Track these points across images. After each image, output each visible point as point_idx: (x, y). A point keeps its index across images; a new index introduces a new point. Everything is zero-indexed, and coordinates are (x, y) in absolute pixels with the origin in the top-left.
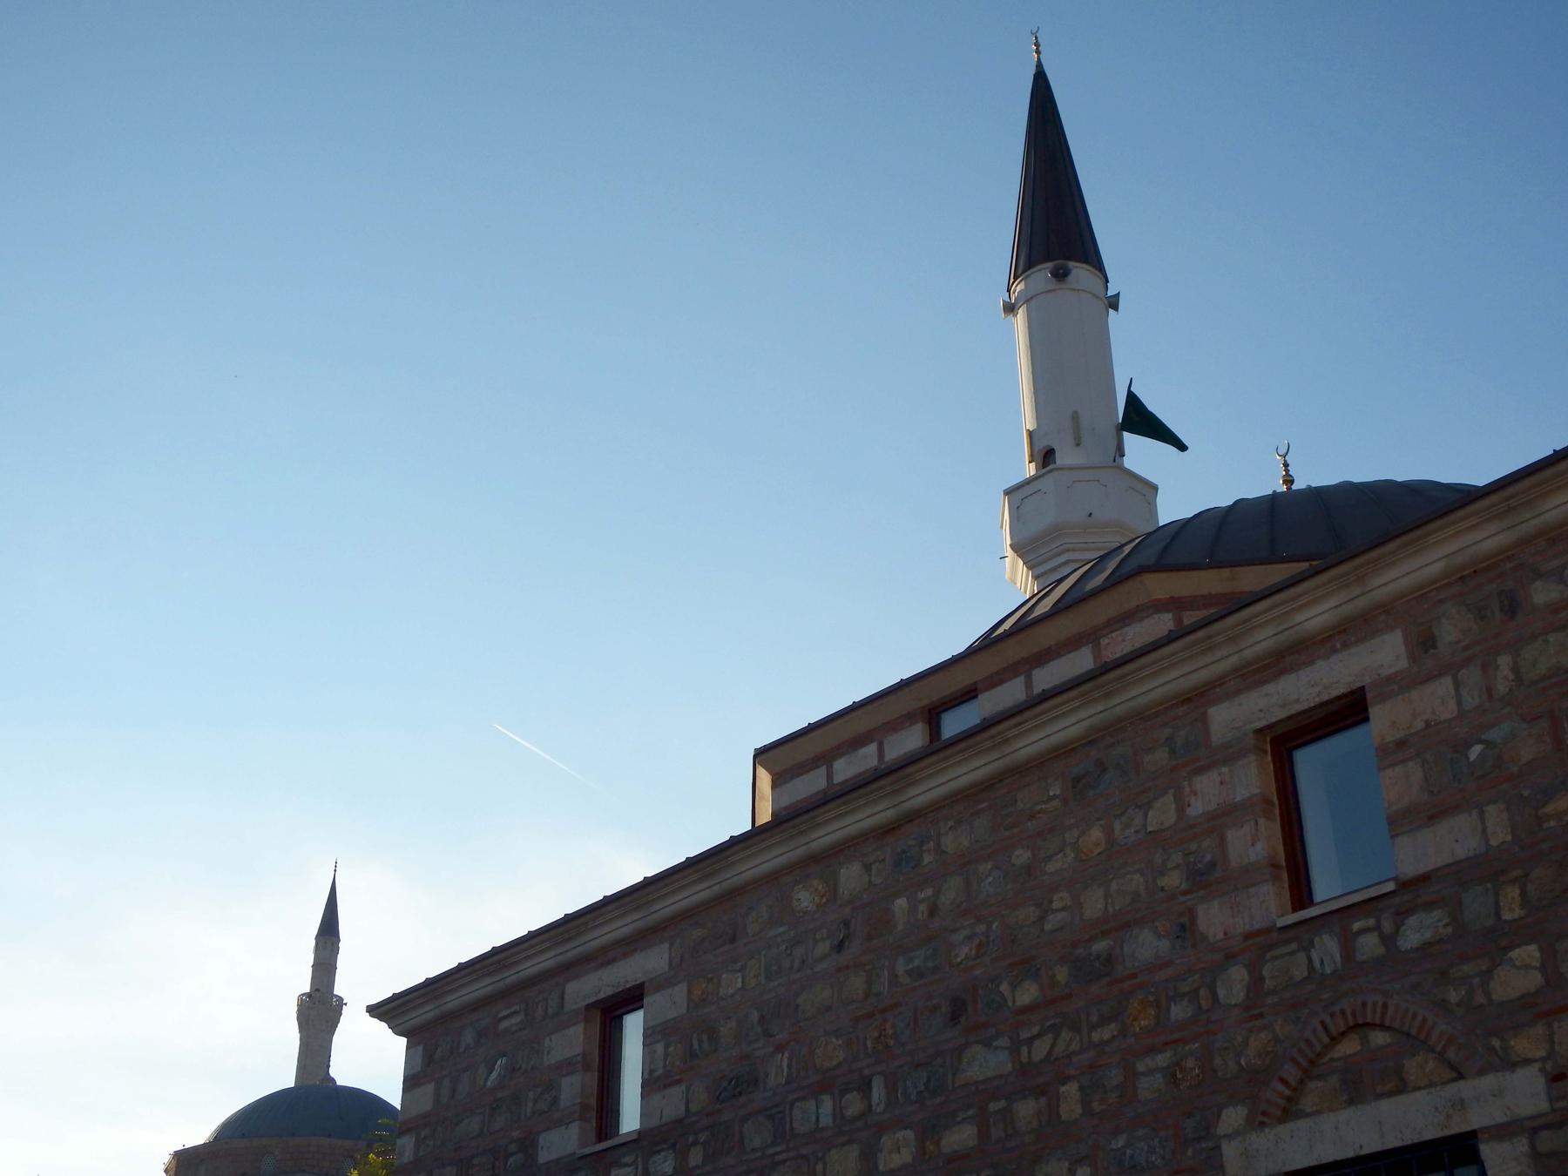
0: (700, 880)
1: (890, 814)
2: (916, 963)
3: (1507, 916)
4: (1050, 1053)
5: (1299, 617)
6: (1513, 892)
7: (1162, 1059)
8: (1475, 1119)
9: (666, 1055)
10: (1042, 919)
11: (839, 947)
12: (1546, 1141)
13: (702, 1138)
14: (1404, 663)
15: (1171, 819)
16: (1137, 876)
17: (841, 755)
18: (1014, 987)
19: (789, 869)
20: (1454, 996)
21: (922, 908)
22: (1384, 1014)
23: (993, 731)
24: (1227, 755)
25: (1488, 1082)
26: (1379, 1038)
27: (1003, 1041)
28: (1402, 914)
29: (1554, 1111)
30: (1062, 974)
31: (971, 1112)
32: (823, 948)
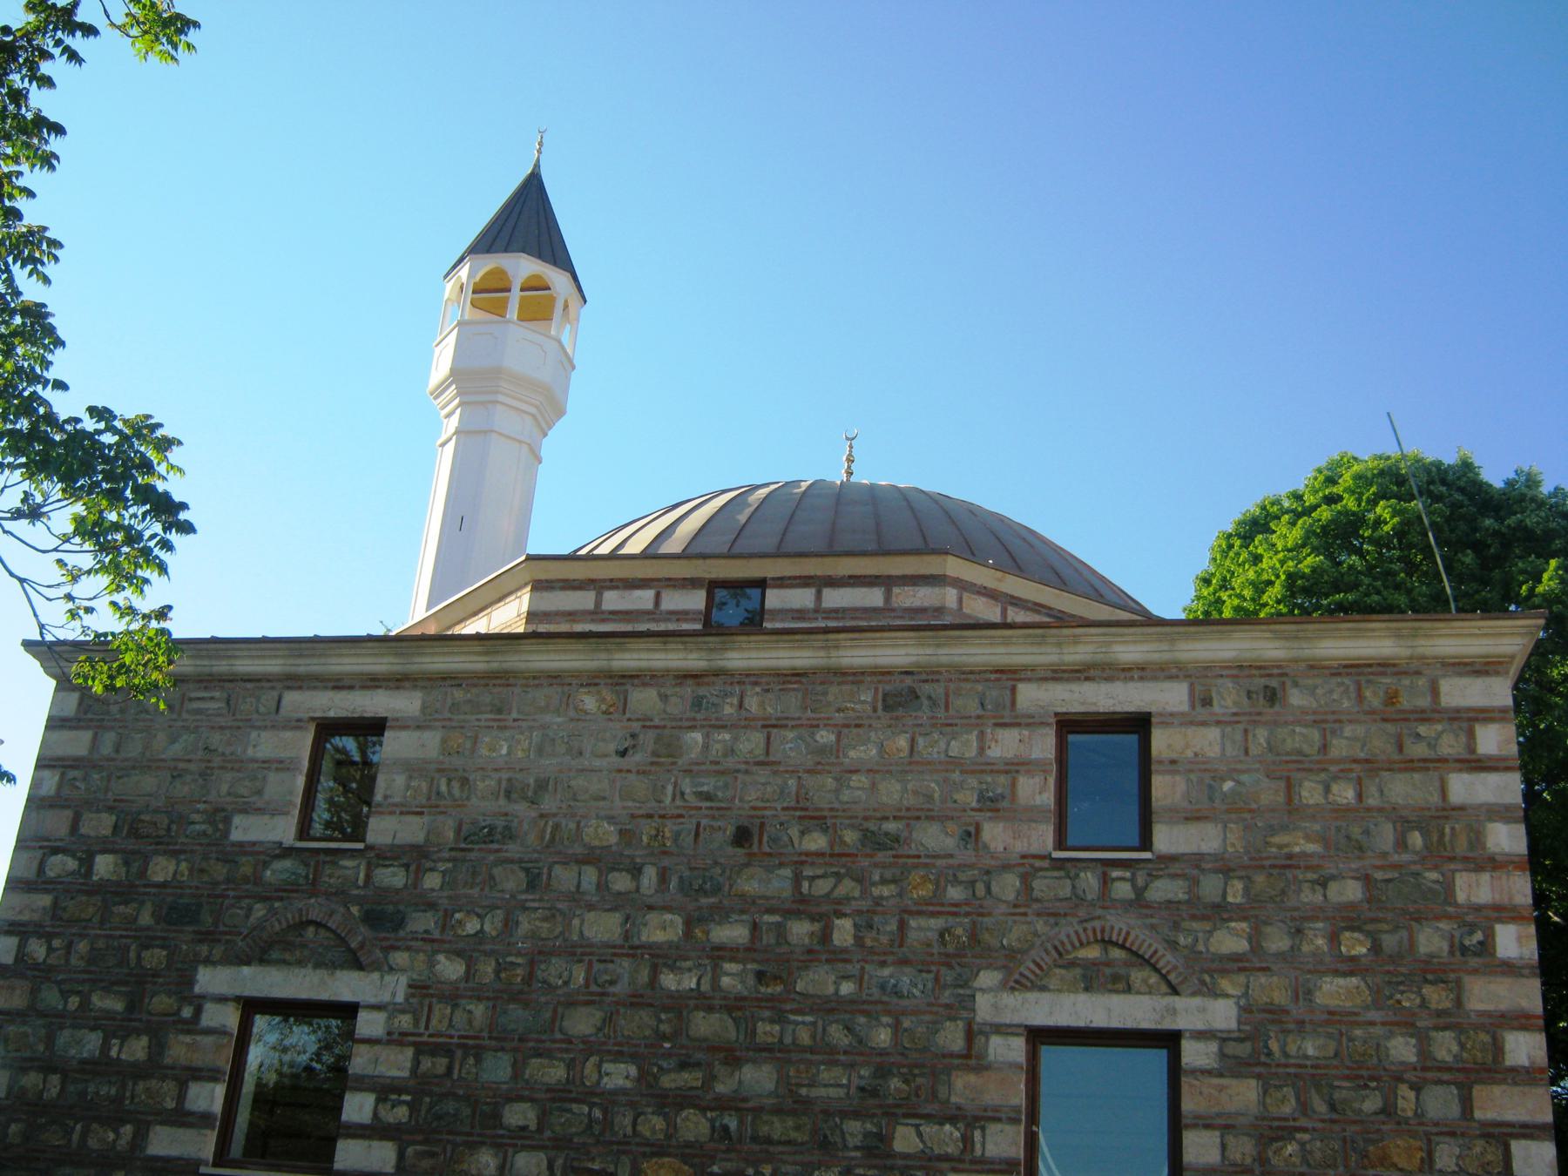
0: (479, 654)
1: (702, 664)
2: (705, 788)
3: (1230, 899)
4: (828, 895)
7: (937, 923)
8: (1180, 1023)
9: (408, 787)
10: (837, 791)
11: (623, 753)
12: (1232, 1048)
13: (442, 866)
14: (1185, 708)
15: (972, 752)
17: (616, 588)
18: (803, 833)
20: (1182, 940)
21: (716, 749)
22: (1125, 939)
23: (831, 636)
26: (1116, 953)
27: (787, 872)
28: (1152, 877)
30: (850, 837)
31: (744, 917)
32: (612, 747)
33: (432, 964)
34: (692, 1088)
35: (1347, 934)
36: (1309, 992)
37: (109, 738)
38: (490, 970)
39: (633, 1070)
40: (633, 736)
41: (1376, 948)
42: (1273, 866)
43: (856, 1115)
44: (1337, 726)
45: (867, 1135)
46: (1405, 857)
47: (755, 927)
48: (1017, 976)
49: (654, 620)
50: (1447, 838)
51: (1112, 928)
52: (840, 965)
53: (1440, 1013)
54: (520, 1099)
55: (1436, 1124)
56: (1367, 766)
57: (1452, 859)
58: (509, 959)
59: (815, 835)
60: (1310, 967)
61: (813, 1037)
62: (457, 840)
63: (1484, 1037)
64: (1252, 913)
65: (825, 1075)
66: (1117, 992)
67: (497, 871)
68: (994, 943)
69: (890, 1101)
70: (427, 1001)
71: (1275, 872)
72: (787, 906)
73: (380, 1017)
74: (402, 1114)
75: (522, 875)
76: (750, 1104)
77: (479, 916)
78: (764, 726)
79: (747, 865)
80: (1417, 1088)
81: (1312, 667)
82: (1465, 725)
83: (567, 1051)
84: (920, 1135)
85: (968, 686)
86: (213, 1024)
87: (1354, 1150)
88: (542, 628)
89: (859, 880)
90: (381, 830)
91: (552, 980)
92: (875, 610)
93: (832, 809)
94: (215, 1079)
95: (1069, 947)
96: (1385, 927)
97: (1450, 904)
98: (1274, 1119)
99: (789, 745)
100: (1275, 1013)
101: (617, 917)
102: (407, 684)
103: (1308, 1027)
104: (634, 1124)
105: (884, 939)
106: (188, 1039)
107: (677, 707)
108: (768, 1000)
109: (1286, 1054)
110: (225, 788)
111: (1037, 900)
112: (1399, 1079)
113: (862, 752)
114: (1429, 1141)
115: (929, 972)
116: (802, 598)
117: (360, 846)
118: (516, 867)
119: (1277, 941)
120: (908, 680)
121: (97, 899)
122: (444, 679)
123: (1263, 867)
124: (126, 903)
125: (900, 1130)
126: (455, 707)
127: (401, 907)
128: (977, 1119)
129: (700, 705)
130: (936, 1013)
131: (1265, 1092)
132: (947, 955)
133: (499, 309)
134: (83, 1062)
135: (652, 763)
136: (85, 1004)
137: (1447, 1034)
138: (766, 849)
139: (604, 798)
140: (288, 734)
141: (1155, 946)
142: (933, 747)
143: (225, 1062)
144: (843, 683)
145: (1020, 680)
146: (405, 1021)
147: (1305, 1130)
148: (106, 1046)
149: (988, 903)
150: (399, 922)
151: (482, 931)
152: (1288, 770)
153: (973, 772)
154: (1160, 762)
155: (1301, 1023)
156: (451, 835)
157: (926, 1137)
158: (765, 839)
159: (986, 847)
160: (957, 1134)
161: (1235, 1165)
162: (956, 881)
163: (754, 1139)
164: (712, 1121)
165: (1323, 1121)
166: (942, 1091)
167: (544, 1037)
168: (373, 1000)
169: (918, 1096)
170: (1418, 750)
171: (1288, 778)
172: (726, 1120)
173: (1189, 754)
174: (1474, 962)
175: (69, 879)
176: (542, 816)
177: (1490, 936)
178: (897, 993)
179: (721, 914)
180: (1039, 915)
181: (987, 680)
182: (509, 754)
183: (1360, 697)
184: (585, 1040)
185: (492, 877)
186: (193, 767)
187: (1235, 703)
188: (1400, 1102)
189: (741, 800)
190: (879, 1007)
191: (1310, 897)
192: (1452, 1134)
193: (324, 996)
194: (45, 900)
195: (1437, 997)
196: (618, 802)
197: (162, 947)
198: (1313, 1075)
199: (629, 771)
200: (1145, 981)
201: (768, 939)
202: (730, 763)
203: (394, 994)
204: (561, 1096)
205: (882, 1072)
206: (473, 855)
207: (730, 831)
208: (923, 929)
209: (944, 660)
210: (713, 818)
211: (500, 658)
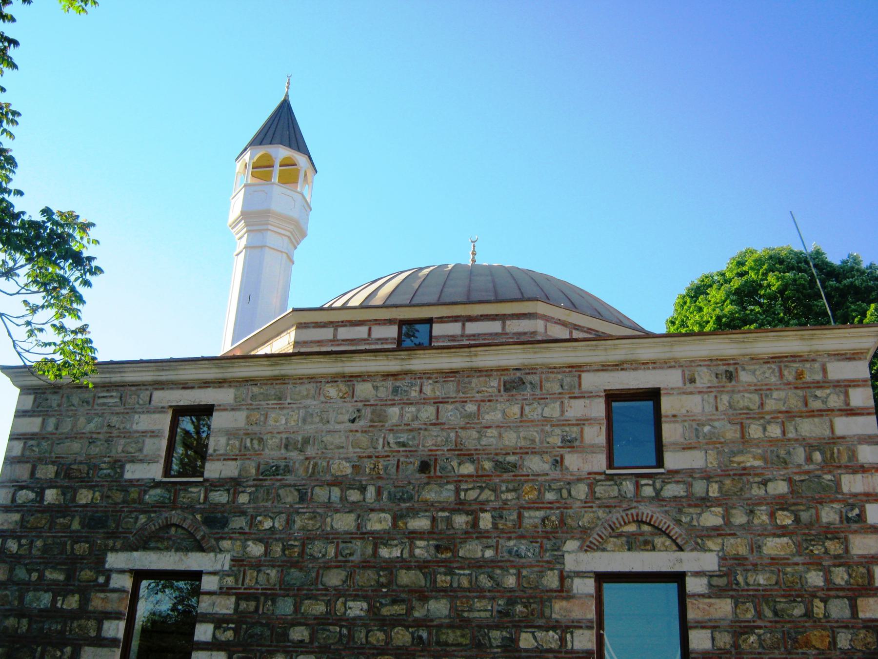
2: (402, 440)
5: (639, 351)
6: (715, 486)
7: (540, 514)
9: (228, 444)
10: (479, 439)
11: (353, 421)
13: (249, 490)
14: (680, 384)
15: (556, 414)
16: (535, 434)
18: (460, 464)
19: (324, 376)
20: (684, 520)
21: (408, 417)
22: (651, 520)
23: (473, 349)
24: (589, 396)
25: (695, 554)
26: (646, 528)
27: (451, 487)
29: (719, 570)
30: (488, 465)
31: (427, 514)
32: (346, 417)
33: (245, 547)
34: (400, 615)
35: (780, 512)
36: (759, 547)
37: (52, 421)
38: (279, 549)
39: (365, 606)
40: (358, 411)
41: (797, 520)
42: (735, 475)
43: (497, 627)
44: (768, 392)
45: (503, 639)
46: (812, 467)
47: (434, 520)
48: (588, 543)
49: (368, 344)
50: (835, 455)
51: (643, 514)
52: (485, 540)
53: (837, 557)
54: (300, 624)
55: (837, 622)
56: (787, 415)
57: (839, 467)
58: (290, 543)
59: (467, 465)
60: (759, 532)
61: (470, 582)
62: (257, 474)
63: (862, 570)
64: (724, 502)
65: (478, 605)
66: (647, 550)
67: (281, 492)
68: (574, 524)
69: (517, 619)
70: (242, 569)
71: (736, 478)
72: (452, 506)
73: (216, 579)
74: (229, 635)
75: (296, 493)
76: (435, 623)
77: (271, 518)
78: (435, 403)
79: (428, 483)
80: (825, 601)
81: (753, 359)
82: (843, 389)
83: (326, 595)
84: (535, 638)
85: (553, 376)
86: (116, 586)
87: (790, 638)
88: (302, 350)
89: (494, 490)
90: (213, 470)
91: (315, 554)
92: (496, 334)
93: (476, 450)
94: (119, 619)
95: (618, 525)
96: (802, 507)
97: (839, 493)
98: (742, 622)
99: (449, 413)
100: (740, 560)
101: (352, 517)
102: (226, 385)
103: (759, 567)
104: (367, 637)
105: (510, 524)
106: (102, 595)
107: (383, 393)
108: (442, 562)
109: (747, 584)
110: (120, 449)
111: (598, 499)
112: (814, 596)
113: (493, 416)
114: (833, 632)
115: (537, 542)
116: (454, 329)
117: (201, 479)
118: (292, 489)
119: (739, 518)
120: (518, 374)
121: (47, 515)
122: (247, 381)
123: (729, 475)
124: (64, 517)
125: (523, 636)
126: (254, 397)
127: (226, 515)
128: (568, 627)
129: (397, 391)
130: (542, 566)
131: (736, 607)
132: (547, 532)
133: (267, 178)
134: (41, 610)
135: (371, 426)
136: (41, 577)
137: (841, 568)
138: (438, 474)
139: (343, 447)
140: (157, 416)
141: (668, 523)
142: (534, 412)
143: (124, 608)
144: (478, 377)
145: (583, 371)
146: (230, 581)
147: (760, 627)
148: (54, 601)
149: (569, 501)
150: (225, 523)
151: (273, 526)
152: (741, 419)
153: (558, 425)
154: (667, 416)
155: (755, 565)
156: (253, 471)
157: (539, 639)
158: (438, 468)
159: (567, 468)
160: (556, 637)
161: (721, 649)
162: (550, 489)
163: (438, 643)
164: (412, 634)
165: (771, 622)
166: (547, 612)
167: (312, 587)
168: (211, 569)
169: (533, 615)
170: (816, 405)
171: (742, 423)
172: (420, 633)
173: (684, 411)
174: (854, 526)
175: (30, 504)
176: (307, 459)
177: (863, 511)
178: (518, 555)
179: (414, 512)
180: (599, 507)
181: (565, 372)
182: (286, 423)
183: (781, 376)
184: (336, 588)
185: (279, 496)
186: (101, 436)
187: (709, 381)
188: (815, 610)
189: (423, 446)
190: (508, 564)
191: (757, 491)
192: (846, 627)
193: (182, 567)
194: (16, 517)
195: (834, 547)
196: (351, 449)
197: (87, 542)
198: (763, 596)
199: (357, 431)
200: (663, 544)
201: (442, 526)
202: (415, 425)
203: (223, 566)
204: (322, 621)
205: (512, 602)
206: (267, 483)
207: (417, 464)
208: (532, 518)
209: (539, 361)
210: (407, 456)
211: (279, 368)
